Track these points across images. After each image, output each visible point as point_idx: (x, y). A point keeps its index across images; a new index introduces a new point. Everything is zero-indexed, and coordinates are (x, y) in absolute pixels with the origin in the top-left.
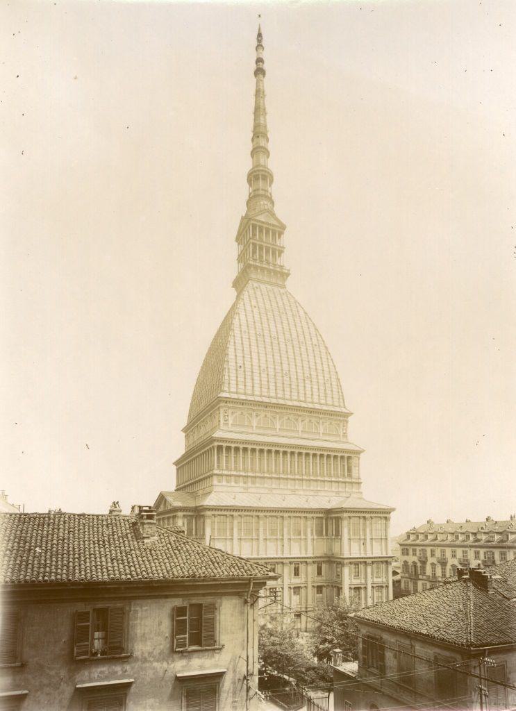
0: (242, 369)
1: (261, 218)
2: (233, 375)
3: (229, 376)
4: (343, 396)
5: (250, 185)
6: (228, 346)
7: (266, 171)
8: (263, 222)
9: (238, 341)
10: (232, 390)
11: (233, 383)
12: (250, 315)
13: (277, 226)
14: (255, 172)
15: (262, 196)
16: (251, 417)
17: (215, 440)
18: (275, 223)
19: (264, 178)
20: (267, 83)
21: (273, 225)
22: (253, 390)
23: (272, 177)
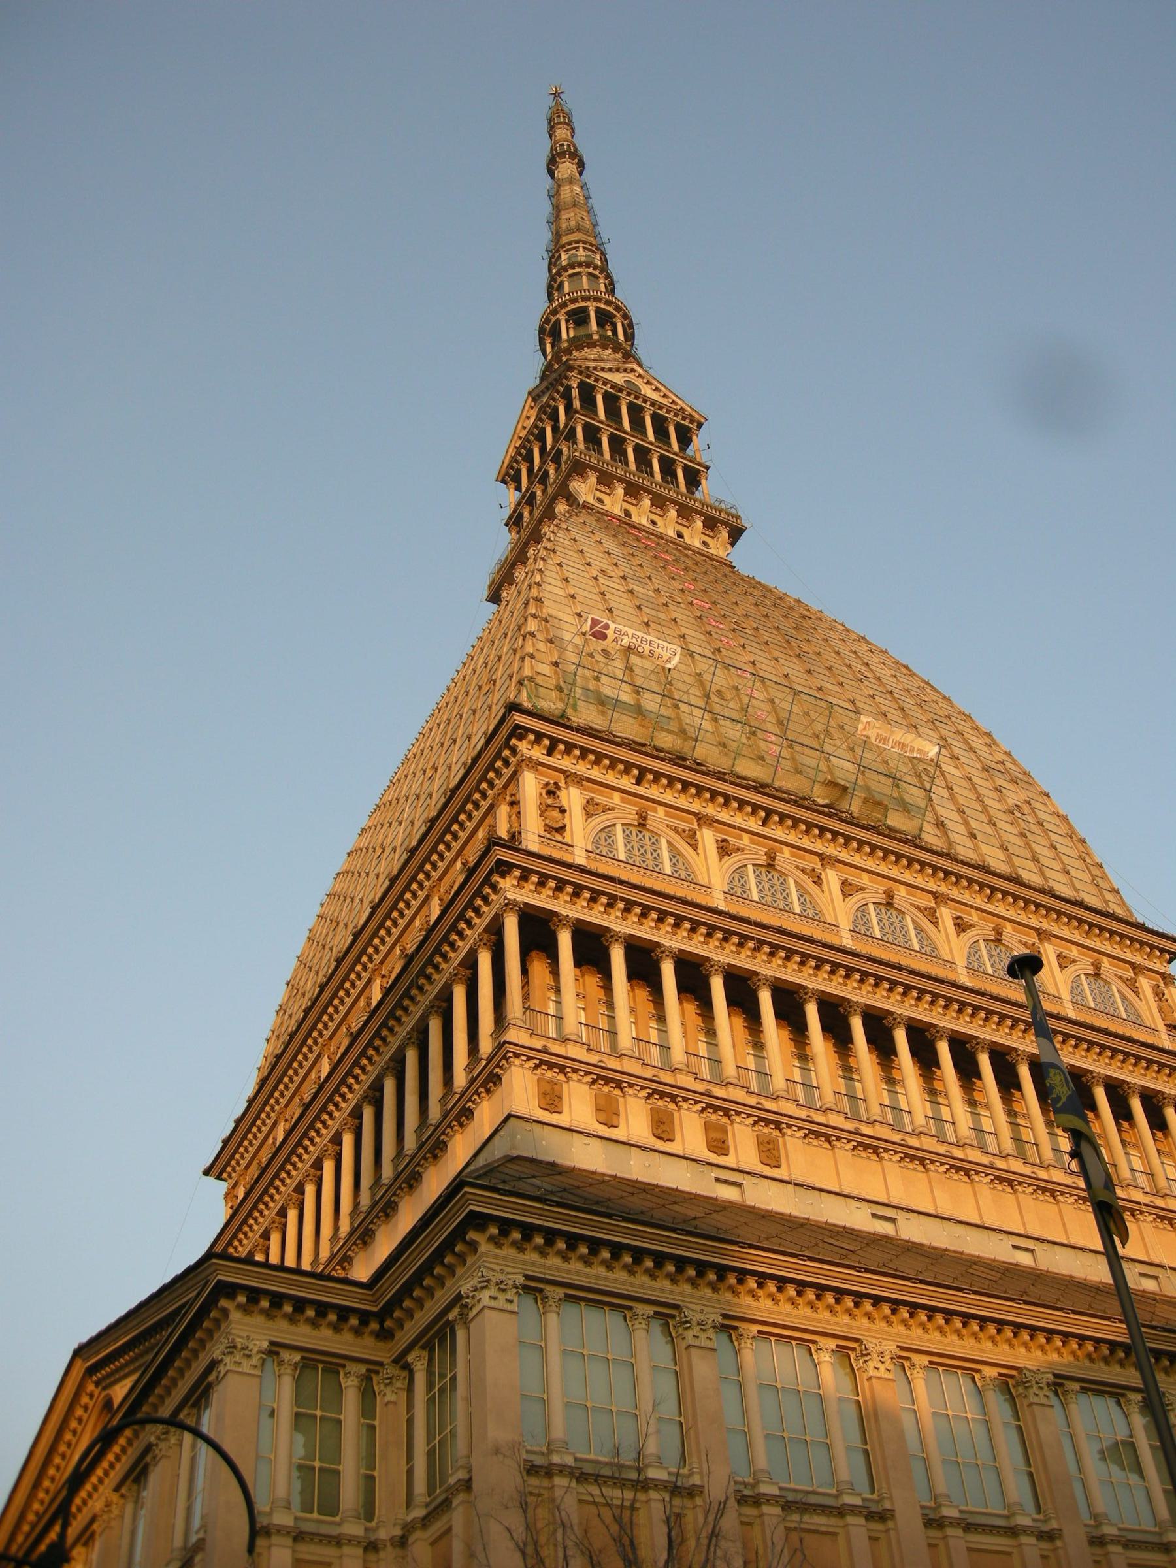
1: (618, 378)
4: (1105, 877)
7: (608, 303)
14: (574, 301)
16: (695, 847)
17: (503, 868)
23: (631, 325)
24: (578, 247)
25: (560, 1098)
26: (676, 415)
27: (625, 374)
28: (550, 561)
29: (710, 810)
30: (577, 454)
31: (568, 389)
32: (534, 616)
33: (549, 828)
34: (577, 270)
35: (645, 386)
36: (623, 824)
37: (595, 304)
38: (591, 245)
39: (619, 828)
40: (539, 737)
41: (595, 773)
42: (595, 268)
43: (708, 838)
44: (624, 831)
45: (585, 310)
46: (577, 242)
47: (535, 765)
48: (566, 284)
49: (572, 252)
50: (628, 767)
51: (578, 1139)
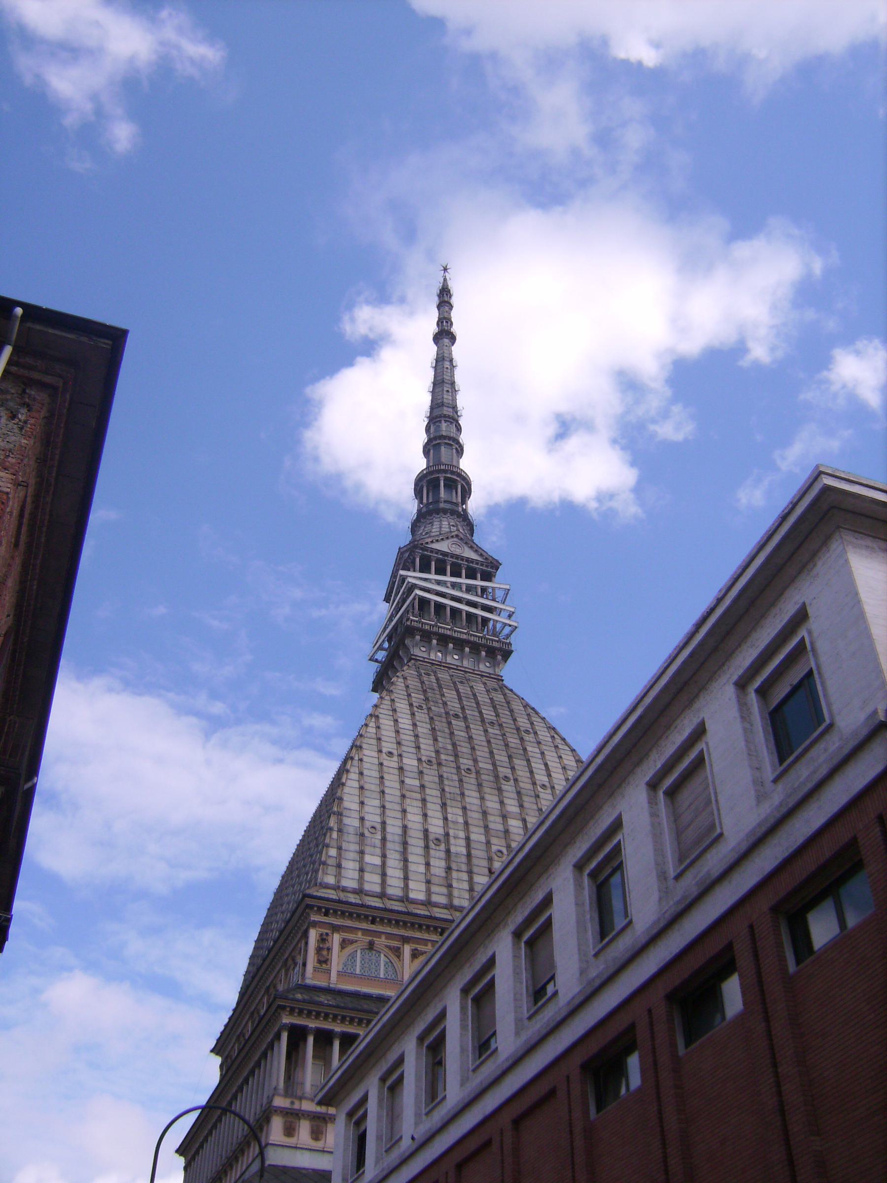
0: (379, 836)
1: (443, 546)
2: (351, 846)
3: (340, 848)
5: (421, 502)
6: (344, 780)
7: (453, 473)
8: (445, 554)
9: (372, 773)
10: (345, 883)
11: (350, 867)
12: (405, 722)
13: (477, 562)
15: (445, 511)
16: (398, 957)
17: (283, 1008)
18: (474, 556)
19: (451, 485)
20: (457, 351)
21: (468, 560)
22: (406, 888)
24: (441, 420)
25: (294, 1130)
26: (482, 565)
27: (453, 540)
28: (356, 758)
29: (409, 933)
30: (409, 623)
31: (414, 559)
32: (334, 814)
33: (320, 962)
34: (438, 441)
35: (464, 545)
36: (361, 949)
37: (444, 475)
38: (449, 417)
39: (359, 952)
40: (320, 908)
41: (348, 923)
42: (450, 438)
43: (407, 950)
44: (361, 953)
45: (438, 479)
46: (440, 416)
47: (315, 924)
48: (432, 451)
49: (437, 424)
50: (366, 917)
51: (298, 1152)
